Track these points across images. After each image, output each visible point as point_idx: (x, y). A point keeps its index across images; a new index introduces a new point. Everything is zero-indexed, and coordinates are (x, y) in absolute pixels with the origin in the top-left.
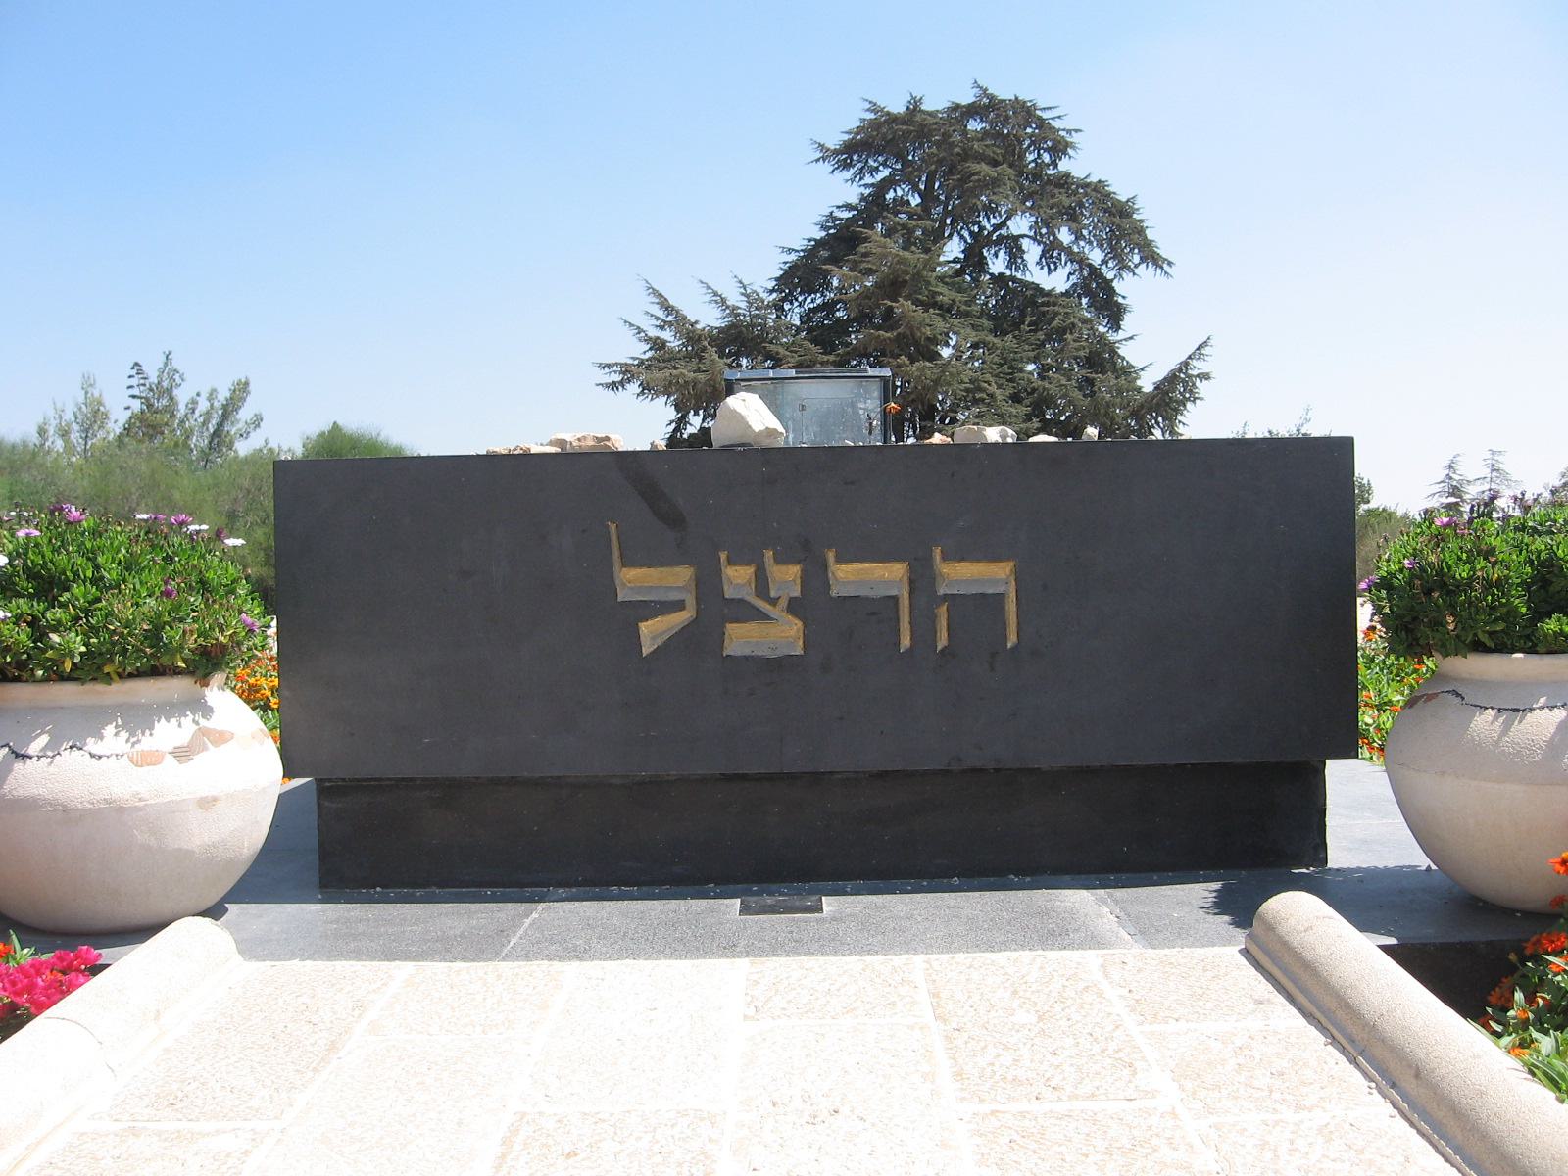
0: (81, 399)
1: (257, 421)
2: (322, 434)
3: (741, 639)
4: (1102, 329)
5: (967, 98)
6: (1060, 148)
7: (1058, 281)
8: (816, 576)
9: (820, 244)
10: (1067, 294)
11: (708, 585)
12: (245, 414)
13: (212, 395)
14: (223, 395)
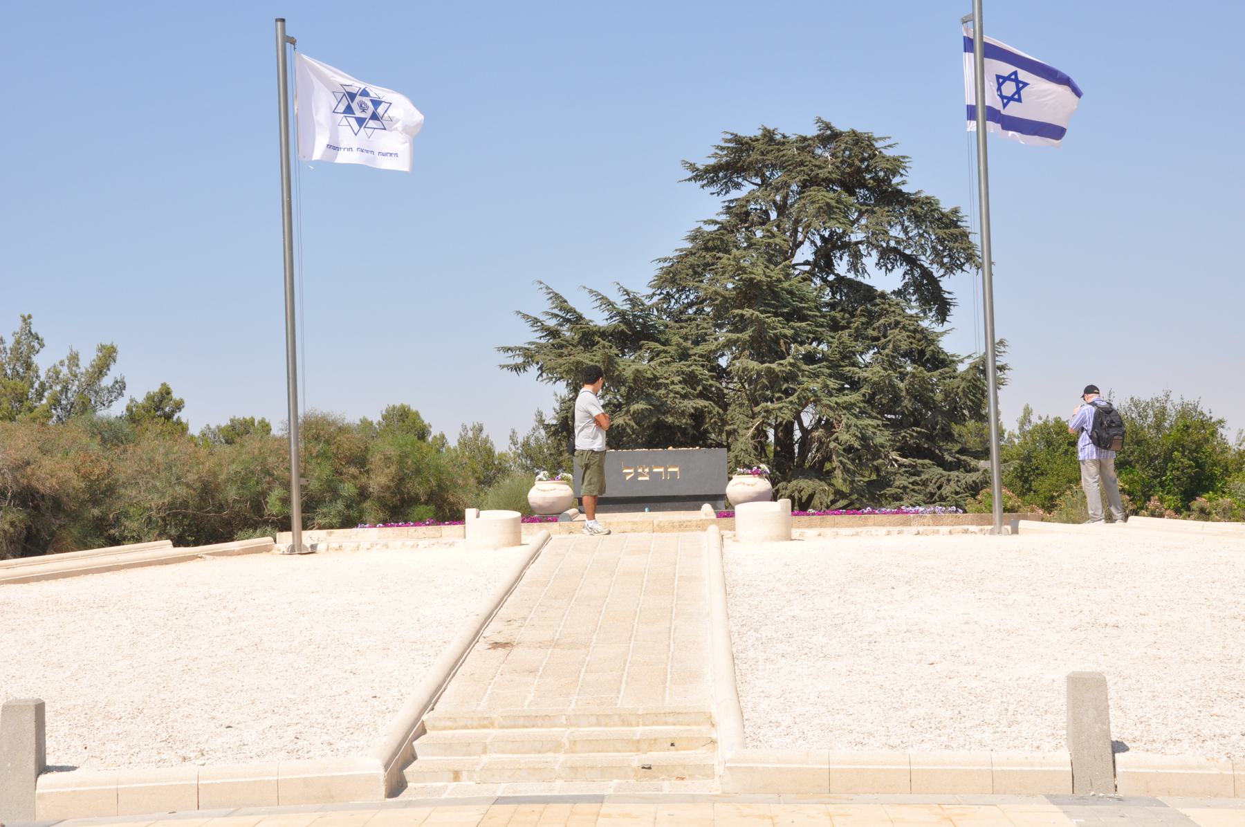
1: (120, 387)
4: (925, 324)
5: (812, 131)
6: (896, 166)
8: (651, 470)
10: (898, 293)
11: (636, 471)
12: (107, 381)
14: (87, 362)
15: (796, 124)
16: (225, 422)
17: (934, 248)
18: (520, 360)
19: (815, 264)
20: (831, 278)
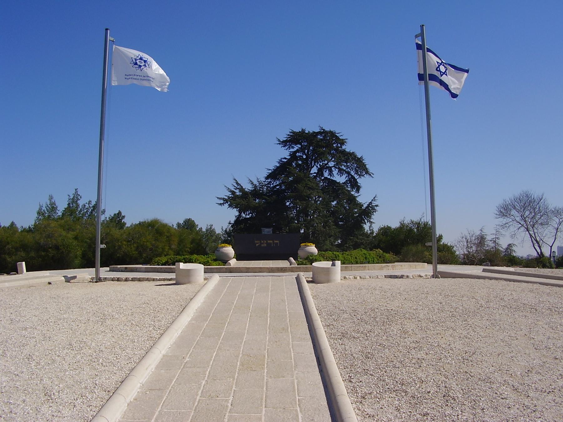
0: (49, 203)
3: (262, 245)
4: (353, 193)
5: (317, 130)
6: (343, 142)
7: (341, 179)
9: (278, 167)
13: (90, 202)
15: (312, 127)
17: (355, 169)
18: (222, 202)
19: (317, 174)
20: (323, 178)
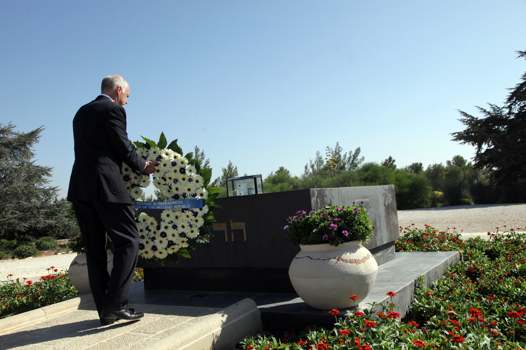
1: (363, 159)
2: (282, 176)
12: (359, 157)
13: (351, 152)
16: (411, 164)
